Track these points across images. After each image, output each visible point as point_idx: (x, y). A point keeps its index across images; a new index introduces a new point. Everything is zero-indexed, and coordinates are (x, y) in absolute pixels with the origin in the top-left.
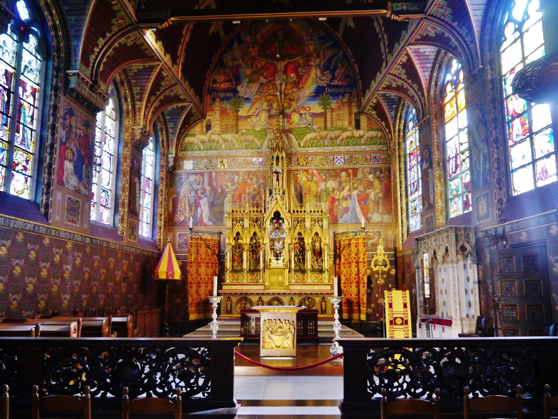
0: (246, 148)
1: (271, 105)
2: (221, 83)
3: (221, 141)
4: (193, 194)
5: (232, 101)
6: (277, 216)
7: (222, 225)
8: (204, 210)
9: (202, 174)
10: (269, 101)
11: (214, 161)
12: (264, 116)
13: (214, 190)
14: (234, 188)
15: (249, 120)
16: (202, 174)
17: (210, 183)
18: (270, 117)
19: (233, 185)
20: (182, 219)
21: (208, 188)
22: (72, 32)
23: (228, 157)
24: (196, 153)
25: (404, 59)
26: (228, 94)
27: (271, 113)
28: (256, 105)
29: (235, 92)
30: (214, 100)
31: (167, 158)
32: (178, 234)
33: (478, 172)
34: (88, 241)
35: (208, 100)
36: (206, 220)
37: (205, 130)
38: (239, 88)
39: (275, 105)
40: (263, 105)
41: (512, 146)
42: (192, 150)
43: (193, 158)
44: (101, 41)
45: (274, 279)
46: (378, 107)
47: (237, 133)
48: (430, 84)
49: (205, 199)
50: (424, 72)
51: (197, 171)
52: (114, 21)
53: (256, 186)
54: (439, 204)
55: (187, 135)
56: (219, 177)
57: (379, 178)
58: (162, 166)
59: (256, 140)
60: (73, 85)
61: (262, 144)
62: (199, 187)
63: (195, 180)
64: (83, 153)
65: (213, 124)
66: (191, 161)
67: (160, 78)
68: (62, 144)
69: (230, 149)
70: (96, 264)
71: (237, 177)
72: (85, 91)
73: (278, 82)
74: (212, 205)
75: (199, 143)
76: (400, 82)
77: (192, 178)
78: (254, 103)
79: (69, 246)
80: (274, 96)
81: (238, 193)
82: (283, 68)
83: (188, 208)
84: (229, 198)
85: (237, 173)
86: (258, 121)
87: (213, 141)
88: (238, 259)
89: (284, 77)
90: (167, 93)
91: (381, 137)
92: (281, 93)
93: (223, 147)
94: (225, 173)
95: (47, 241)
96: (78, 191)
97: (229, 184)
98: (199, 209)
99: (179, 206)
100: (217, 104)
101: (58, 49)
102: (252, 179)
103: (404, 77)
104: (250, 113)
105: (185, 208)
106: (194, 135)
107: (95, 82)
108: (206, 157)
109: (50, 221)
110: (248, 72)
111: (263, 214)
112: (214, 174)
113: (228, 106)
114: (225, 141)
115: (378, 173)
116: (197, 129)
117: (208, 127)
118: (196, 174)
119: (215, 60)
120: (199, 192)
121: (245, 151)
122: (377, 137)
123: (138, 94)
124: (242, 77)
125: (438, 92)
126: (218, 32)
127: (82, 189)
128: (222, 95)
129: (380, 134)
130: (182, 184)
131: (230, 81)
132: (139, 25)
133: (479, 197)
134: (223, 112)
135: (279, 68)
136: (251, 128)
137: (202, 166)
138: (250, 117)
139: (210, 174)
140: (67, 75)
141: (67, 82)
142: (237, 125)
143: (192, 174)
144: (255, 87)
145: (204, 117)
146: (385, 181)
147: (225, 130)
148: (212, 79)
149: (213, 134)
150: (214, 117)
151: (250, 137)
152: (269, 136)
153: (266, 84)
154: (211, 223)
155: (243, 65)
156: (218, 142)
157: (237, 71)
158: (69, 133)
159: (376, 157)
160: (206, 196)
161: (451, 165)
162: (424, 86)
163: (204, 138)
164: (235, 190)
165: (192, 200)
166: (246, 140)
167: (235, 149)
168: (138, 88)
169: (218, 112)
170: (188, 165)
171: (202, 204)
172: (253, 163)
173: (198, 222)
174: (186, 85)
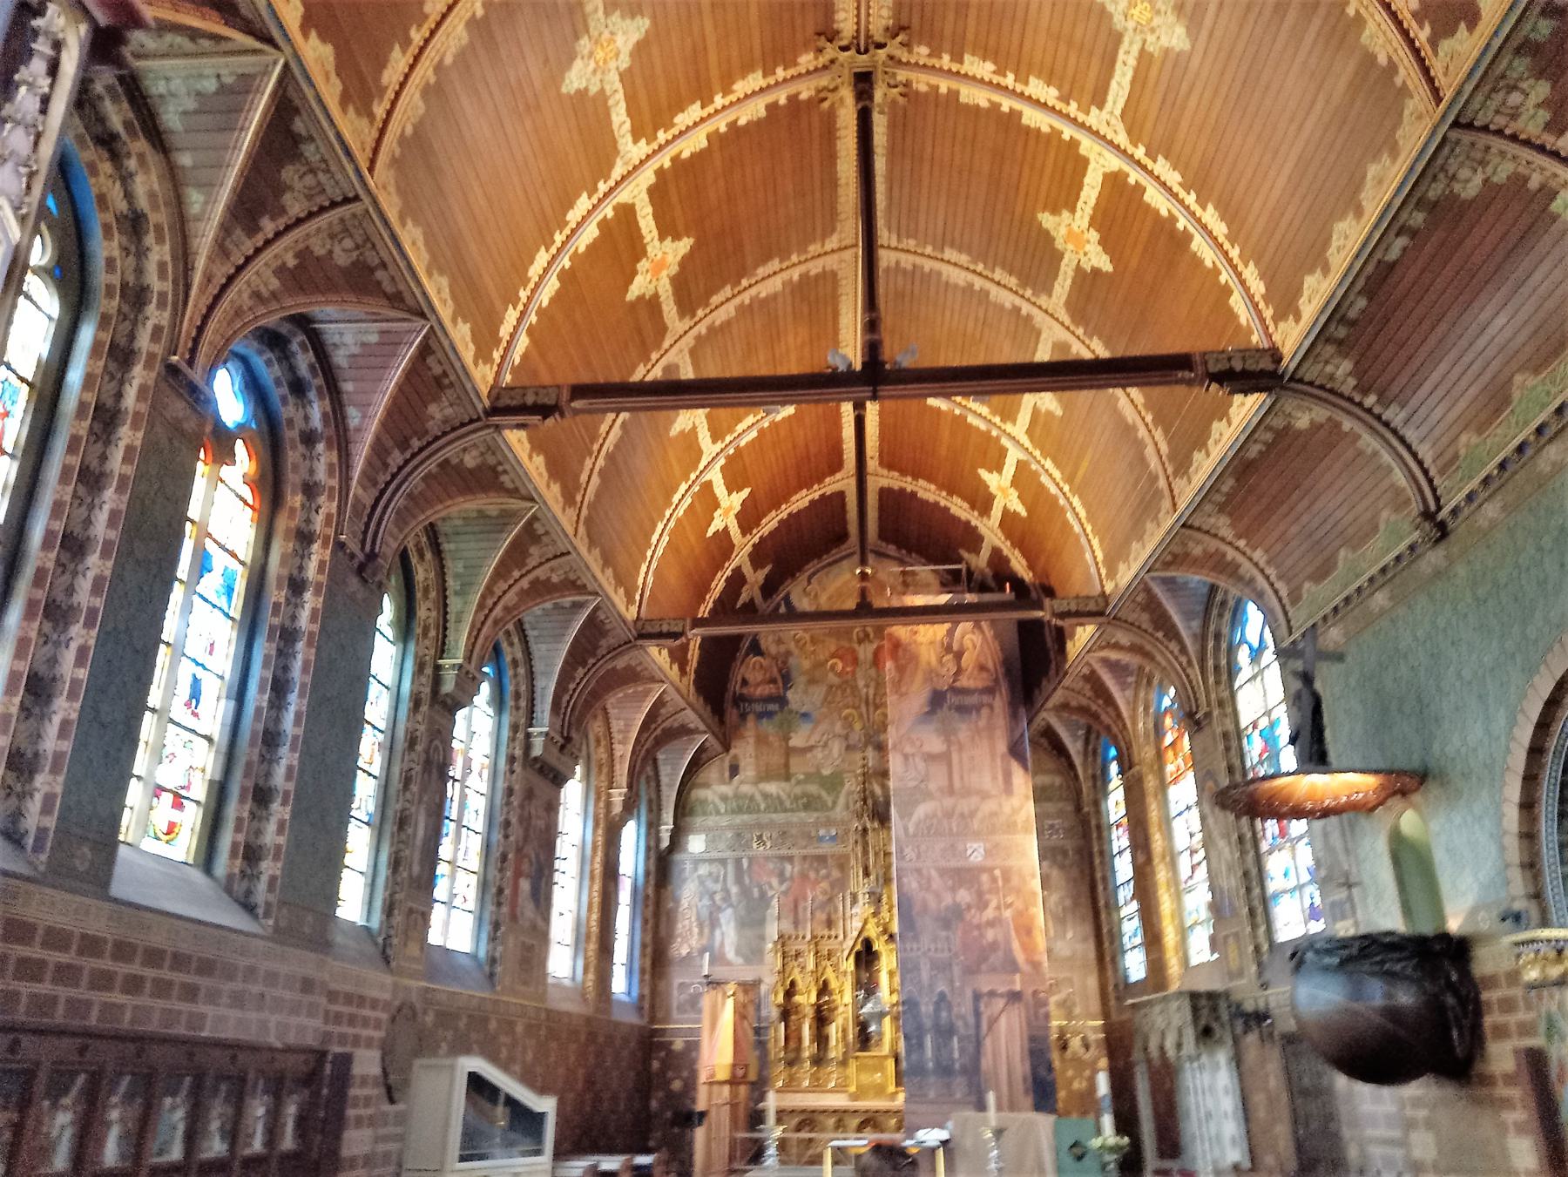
0: (807, 807)
1: (851, 726)
2: (758, 685)
3: (758, 797)
4: (706, 902)
5: (777, 718)
6: (868, 944)
7: (761, 961)
8: (728, 935)
9: (723, 862)
10: (846, 718)
11: (748, 836)
12: (836, 747)
13: (745, 892)
14: (784, 888)
15: (809, 755)
16: (723, 862)
17: (739, 880)
18: (848, 748)
19: (781, 882)
20: (684, 951)
21: (734, 890)
22: (538, 666)
23: (771, 825)
24: (711, 821)
25: (1086, 671)
26: (772, 707)
27: (851, 742)
28: (823, 727)
29: (782, 701)
30: (743, 716)
31: (658, 832)
32: (677, 981)
33: (1221, 889)
34: (543, 1016)
35: (732, 715)
36: (730, 954)
37: (727, 774)
38: (790, 695)
39: (858, 726)
40: (833, 724)
41: (1270, 852)
42: (705, 814)
43: (707, 830)
44: (581, 671)
45: (866, 1078)
46: (1049, 734)
47: (787, 778)
48: (1134, 710)
49: (729, 911)
50: (1123, 690)
51: (714, 855)
52: (603, 643)
53: (825, 885)
54: (1170, 937)
55: (694, 786)
56: (755, 868)
57: (1062, 867)
58: (648, 849)
59: (824, 794)
60: (537, 751)
61: (835, 803)
62: (718, 887)
63: (710, 874)
64: (542, 857)
65: (742, 764)
66: (703, 837)
67: (660, 703)
68: (519, 850)
69: (775, 811)
70: (552, 1059)
71: (788, 867)
72: (554, 759)
73: (861, 683)
74: (742, 924)
75: (717, 801)
76: (1084, 702)
77: (703, 870)
78: (817, 723)
79: (519, 1029)
80: (854, 707)
81: (791, 898)
82: (870, 656)
83: (696, 930)
84: (774, 909)
85: (790, 859)
86: (826, 757)
87: (745, 796)
88: (793, 1037)
89: (873, 672)
90: (667, 724)
91: (1061, 786)
92: (867, 703)
93: (763, 806)
94: (767, 859)
95: (493, 1025)
96: (534, 927)
97: (775, 882)
98: (718, 933)
99: (680, 926)
100: (751, 722)
101: (517, 696)
102: (817, 871)
103: (1089, 694)
104: (812, 742)
105: (690, 929)
106: (707, 785)
107: (568, 739)
108: (729, 827)
109: (498, 988)
110: (806, 664)
111: (841, 943)
112: (745, 863)
113: (768, 727)
114: (766, 796)
115: (1059, 858)
116: (713, 772)
117: (734, 770)
118: (711, 861)
119: (746, 644)
120: (718, 897)
121: (803, 814)
122: (1052, 786)
123: (620, 731)
124: (794, 674)
125: (1151, 725)
126: (752, 600)
127: (540, 923)
128: (758, 708)
129: (1058, 780)
130: (684, 880)
131: (773, 681)
132: (640, 642)
133: (1226, 937)
134: (761, 740)
135: (861, 656)
136: (812, 770)
137: (722, 846)
138: (810, 749)
139: (738, 861)
140: (528, 736)
141: (528, 747)
142: (787, 765)
143: (705, 861)
144: (818, 692)
145: (727, 748)
146: (1075, 872)
147: (765, 776)
148: (739, 679)
149: (742, 782)
150: (745, 750)
151: (813, 789)
152: (847, 786)
153: (839, 687)
154: (740, 960)
155: (796, 652)
156: (752, 798)
157: (785, 663)
158: (527, 830)
159: (1052, 826)
160: (731, 905)
161: (1184, 864)
162: (1125, 713)
163: (726, 789)
164: (785, 893)
165: (705, 913)
166: (805, 795)
167: (785, 811)
168: (622, 723)
169: (751, 740)
170: (696, 844)
171: (723, 921)
172: (821, 839)
173: (719, 958)
174: (699, 702)
